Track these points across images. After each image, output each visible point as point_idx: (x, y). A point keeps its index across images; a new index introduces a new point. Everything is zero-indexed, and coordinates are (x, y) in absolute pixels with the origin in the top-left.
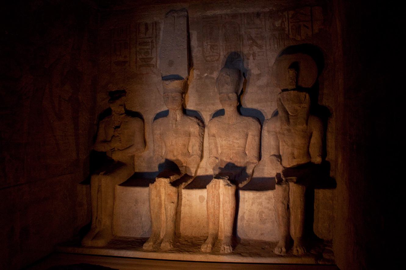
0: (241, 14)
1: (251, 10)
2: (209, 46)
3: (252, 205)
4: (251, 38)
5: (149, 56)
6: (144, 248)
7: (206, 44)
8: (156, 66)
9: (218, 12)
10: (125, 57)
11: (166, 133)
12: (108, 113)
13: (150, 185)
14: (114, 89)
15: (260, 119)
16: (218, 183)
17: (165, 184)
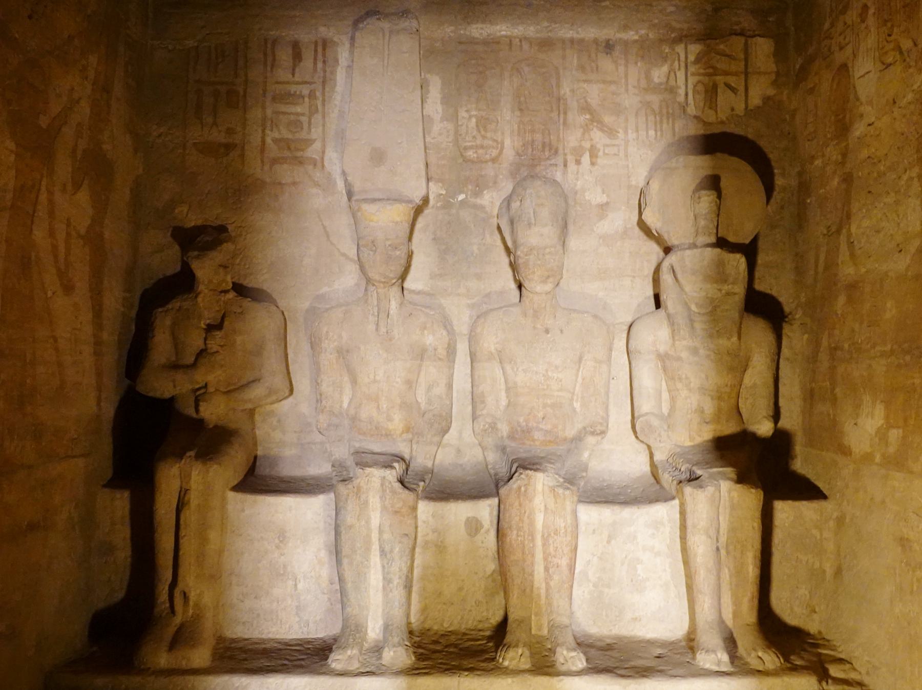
0: (563, 41)
2: (474, 120)
3: (609, 542)
4: (586, 108)
5: (303, 135)
7: (465, 115)
8: (323, 166)
9: (502, 29)
10: (230, 131)
11: (359, 348)
12: (183, 283)
14: (193, 220)
17: (382, 485)
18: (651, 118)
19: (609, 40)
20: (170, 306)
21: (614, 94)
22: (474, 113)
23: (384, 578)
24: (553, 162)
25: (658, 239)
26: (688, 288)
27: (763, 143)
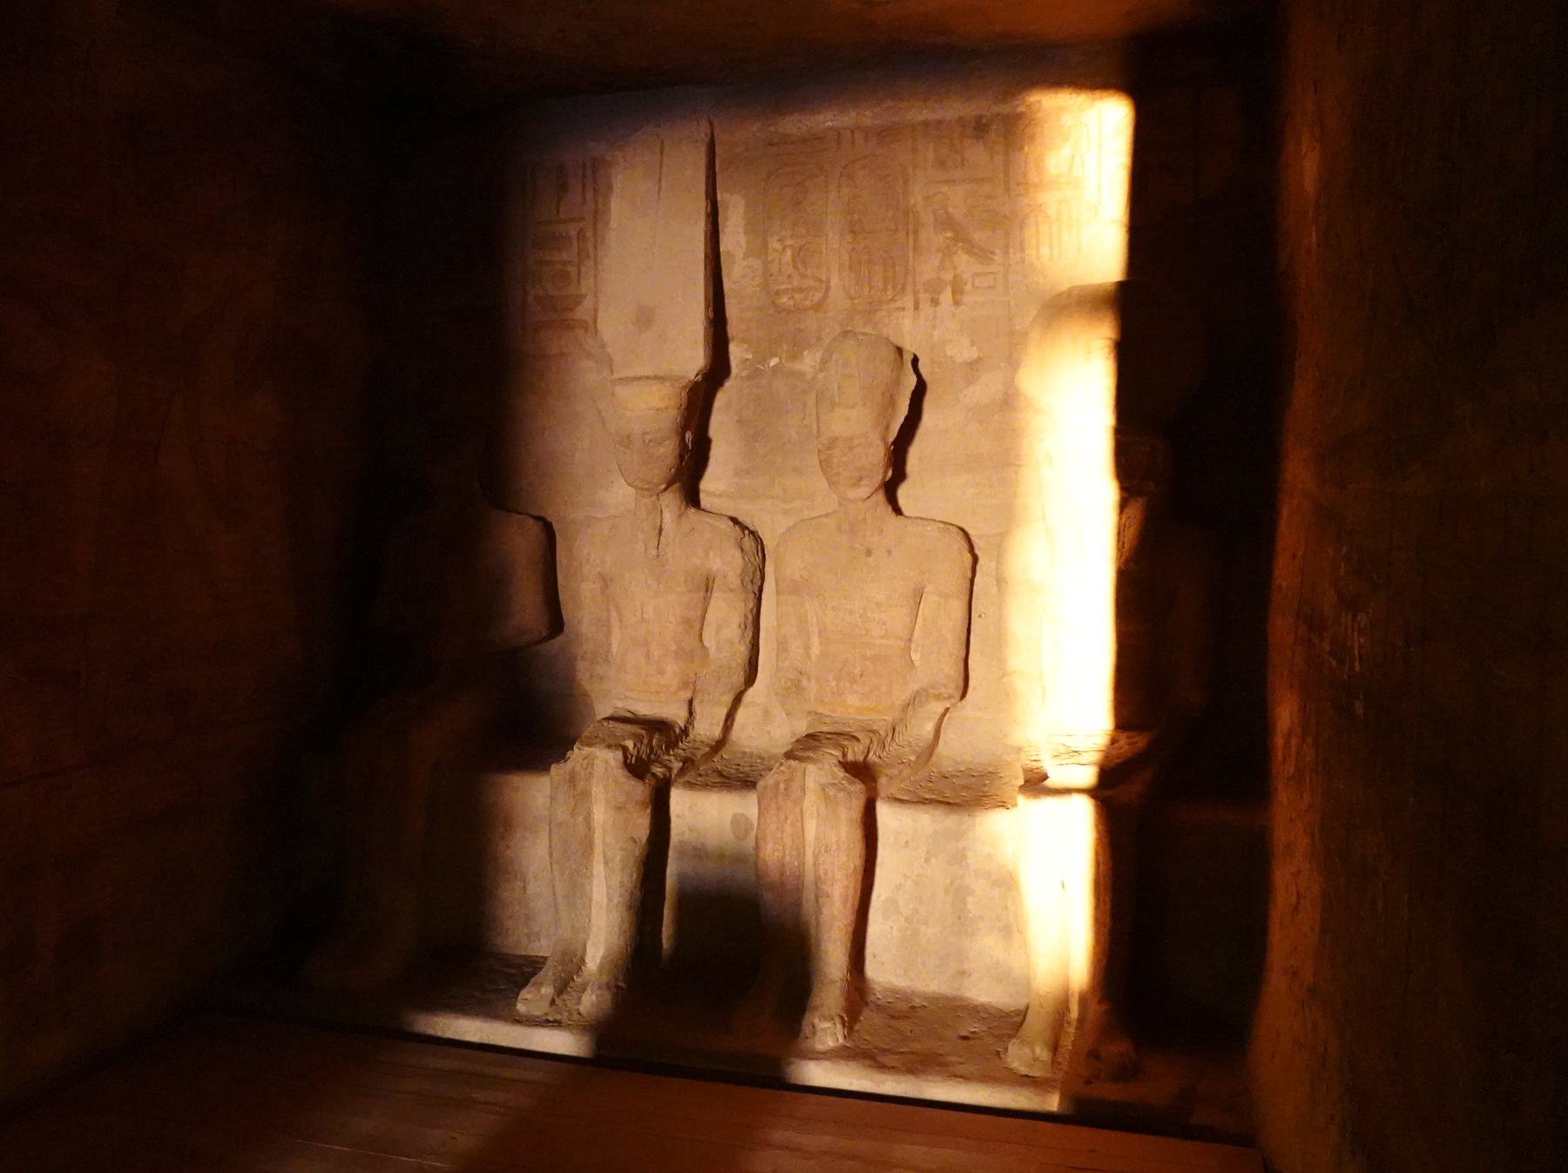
0: (913, 127)
2: (789, 252)
6: (521, 1007)
7: (778, 246)
9: (828, 119)
13: (554, 768)
15: (971, 532)
16: (799, 774)
19: (981, 117)
21: (989, 197)
22: (789, 242)
24: (898, 304)
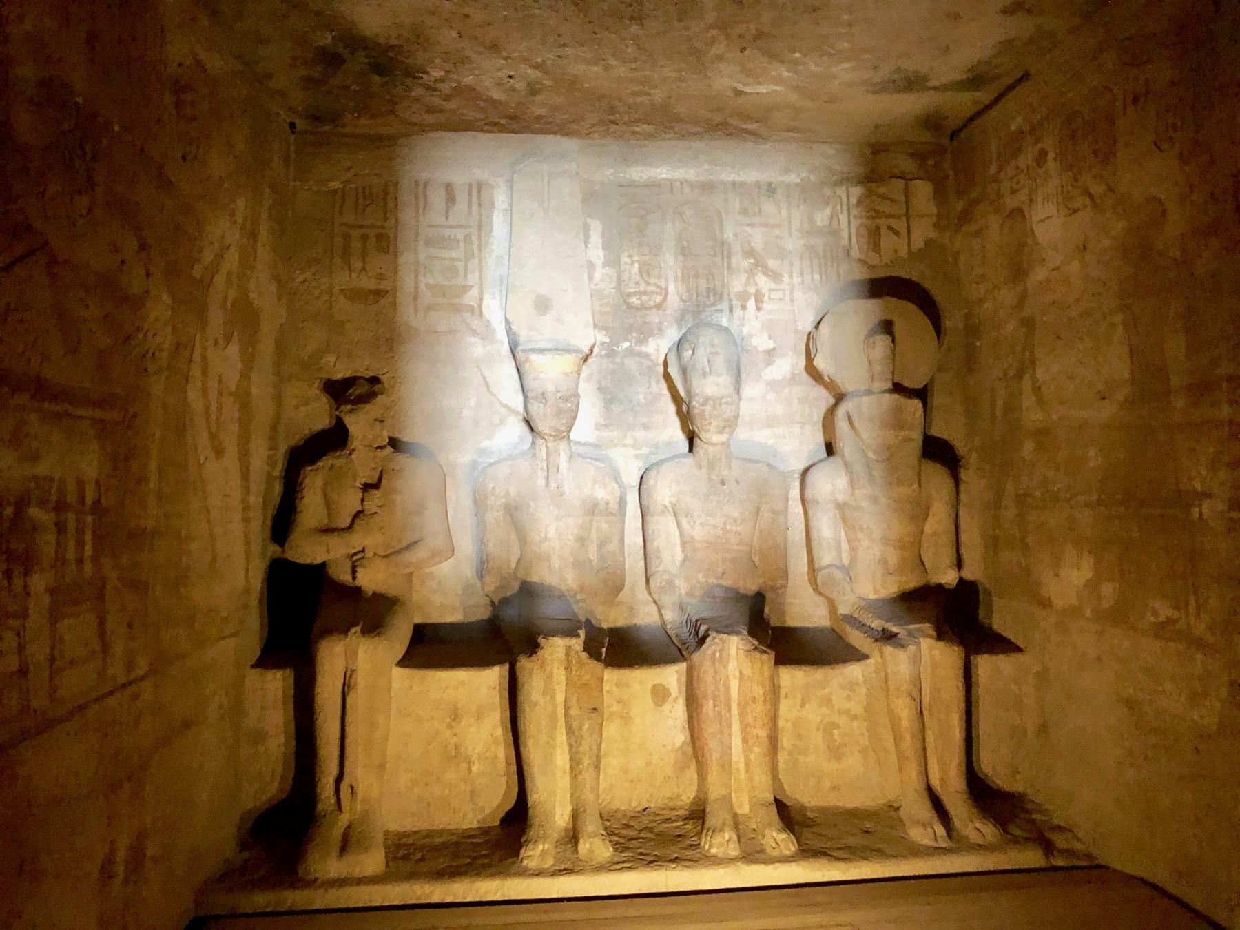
0: (724, 184)
1: (751, 176)
2: (636, 265)
3: (803, 705)
4: (749, 252)
8: (481, 314)
10: (381, 277)
12: (334, 439)
14: (341, 373)
17: (567, 655)
18: (815, 262)
19: (770, 184)
20: (320, 464)
22: (636, 258)
23: (571, 759)
25: (830, 386)
26: (865, 436)
27: (927, 285)
